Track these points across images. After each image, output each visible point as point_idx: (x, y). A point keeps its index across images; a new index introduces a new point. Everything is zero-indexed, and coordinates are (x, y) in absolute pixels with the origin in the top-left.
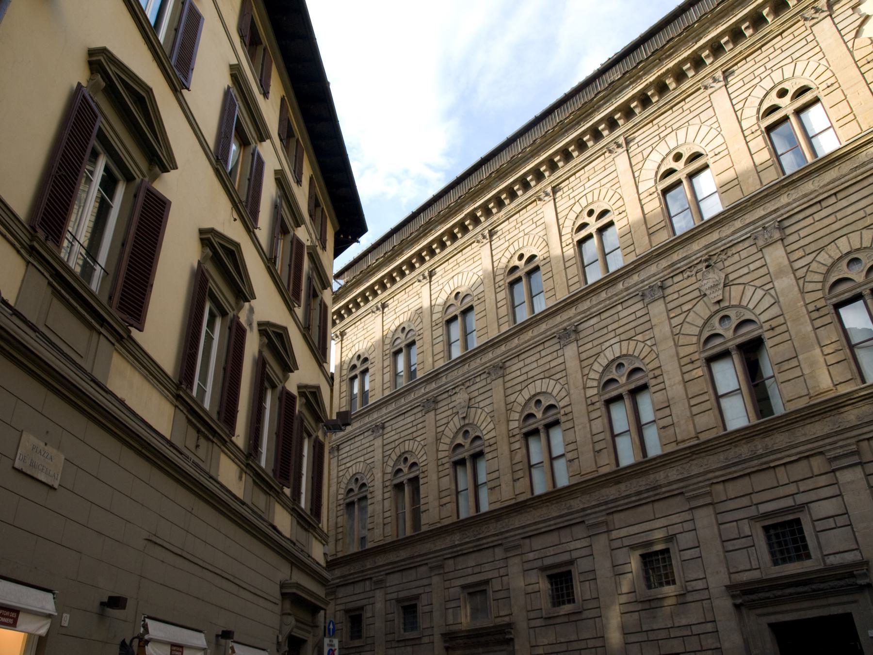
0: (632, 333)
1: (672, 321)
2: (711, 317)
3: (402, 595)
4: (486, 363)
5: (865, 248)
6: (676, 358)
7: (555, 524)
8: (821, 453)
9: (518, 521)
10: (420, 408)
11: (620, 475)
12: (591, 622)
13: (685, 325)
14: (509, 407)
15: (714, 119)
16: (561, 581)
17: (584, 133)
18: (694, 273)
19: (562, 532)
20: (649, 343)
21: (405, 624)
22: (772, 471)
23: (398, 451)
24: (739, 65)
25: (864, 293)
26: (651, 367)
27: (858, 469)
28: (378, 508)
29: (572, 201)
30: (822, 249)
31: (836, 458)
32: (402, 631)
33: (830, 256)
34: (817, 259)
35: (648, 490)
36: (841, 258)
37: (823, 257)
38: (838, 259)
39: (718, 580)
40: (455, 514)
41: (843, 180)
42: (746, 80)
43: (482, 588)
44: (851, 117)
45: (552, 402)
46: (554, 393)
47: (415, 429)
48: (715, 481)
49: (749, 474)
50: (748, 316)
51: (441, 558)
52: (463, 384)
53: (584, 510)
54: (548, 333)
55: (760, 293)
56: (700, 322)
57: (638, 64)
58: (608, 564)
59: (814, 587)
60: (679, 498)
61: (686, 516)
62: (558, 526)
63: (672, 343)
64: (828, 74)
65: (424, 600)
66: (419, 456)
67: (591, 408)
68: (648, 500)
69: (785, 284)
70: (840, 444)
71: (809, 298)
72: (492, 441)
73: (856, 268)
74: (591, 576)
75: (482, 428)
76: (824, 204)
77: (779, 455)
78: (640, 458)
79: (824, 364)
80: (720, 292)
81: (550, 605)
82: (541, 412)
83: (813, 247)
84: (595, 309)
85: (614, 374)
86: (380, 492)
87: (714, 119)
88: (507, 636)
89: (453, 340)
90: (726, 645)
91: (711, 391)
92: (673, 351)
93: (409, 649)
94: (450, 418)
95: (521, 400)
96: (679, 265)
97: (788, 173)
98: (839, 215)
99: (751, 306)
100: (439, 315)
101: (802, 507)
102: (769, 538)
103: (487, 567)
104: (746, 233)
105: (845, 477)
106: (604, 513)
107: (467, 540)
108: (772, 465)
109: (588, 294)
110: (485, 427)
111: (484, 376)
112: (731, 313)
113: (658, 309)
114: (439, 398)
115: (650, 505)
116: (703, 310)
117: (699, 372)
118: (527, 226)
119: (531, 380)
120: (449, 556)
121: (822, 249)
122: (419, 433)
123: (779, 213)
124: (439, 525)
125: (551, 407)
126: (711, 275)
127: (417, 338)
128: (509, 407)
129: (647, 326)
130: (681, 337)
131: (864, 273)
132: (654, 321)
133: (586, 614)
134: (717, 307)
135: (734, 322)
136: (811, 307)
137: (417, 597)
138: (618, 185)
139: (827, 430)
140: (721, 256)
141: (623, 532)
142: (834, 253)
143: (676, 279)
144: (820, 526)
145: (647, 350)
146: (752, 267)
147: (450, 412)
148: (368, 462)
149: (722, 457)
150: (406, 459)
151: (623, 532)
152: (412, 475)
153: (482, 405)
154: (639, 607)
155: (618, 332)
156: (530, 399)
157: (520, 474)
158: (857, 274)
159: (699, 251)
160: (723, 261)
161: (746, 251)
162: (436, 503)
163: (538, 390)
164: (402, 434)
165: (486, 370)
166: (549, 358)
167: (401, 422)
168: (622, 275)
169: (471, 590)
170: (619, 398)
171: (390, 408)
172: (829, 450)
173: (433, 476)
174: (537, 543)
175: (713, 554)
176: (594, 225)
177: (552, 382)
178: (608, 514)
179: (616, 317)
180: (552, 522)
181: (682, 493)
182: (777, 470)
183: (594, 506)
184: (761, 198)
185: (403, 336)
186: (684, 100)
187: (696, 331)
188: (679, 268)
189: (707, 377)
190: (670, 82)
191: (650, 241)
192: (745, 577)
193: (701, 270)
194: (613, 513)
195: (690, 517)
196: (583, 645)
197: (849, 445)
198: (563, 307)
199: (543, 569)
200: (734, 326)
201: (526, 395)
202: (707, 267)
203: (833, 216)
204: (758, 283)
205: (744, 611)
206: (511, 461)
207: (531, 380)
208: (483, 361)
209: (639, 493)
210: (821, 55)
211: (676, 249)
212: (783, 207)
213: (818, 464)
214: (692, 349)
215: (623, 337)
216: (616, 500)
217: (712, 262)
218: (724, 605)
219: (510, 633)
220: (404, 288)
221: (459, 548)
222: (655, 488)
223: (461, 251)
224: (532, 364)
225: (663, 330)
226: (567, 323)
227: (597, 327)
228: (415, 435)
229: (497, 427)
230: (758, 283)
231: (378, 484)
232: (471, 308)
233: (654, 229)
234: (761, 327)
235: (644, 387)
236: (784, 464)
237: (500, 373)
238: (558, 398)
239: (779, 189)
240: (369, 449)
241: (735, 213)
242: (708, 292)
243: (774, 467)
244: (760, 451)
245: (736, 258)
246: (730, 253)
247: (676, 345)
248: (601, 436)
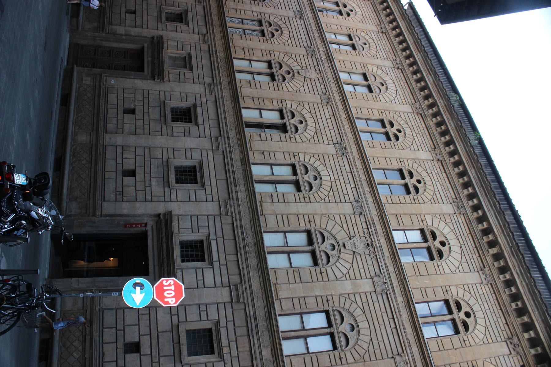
0: (335, 190)
1: (338, 216)
2: (336, 239)
3: (190, 14)
4: (332, 93)
5: (359, 336)
6: (314, 212)
7: (222, 118)
8: (241, 282)
9: (227, 94)
10: (309, 45)
11: (246, 163)
12: (159, 128)
13: (334, 223)
14: (301, 103)
15: (462, 271)
16: (185, 115)
17: (474, 188)
18: (366, 235)
19: (216, 122)
20: (327, 198)
21: (171, 13)
22: (235, 253)
23: (283, 26)
24: (493, 295)
25: (332, 328)
26: (311, 196)
27: (228, 300)
28: (247, 7)
29: (429, 171)
30: (364, 312)
32: (166, 11)
33: (358, 316)
34: (358, 308)
35: (234, 178)
36: (356, 321)
37: (358, 312)
38: (355, 320)
39: (176, 208)
40: (236, 57)
41: (404, 334)
42: (482, 296)
43: (188, 65)
44: (441, 348)
45: (300, 131)
46: (305, 133)
47: (296, 39)
48: (234, 219)
49: (235, 239)
50: (332, 261)
51: (210, 43)
52: (321, 76)
53: (228, 137)
54: (345, 137)
55: (345, 271)
56: (334, 232)
57: (512, 233)
58: (192, 146)
59: (165, 260)
60: (227, 196)
61: (216, 198)
62: (220, 119)
63: (324, 213)
64: (472, 343)
65: (185, 28)
66: (278, 39)
67: (292, 154)
68: (228, 178)
69: (347, 287)
70: (245, 294)
71: (336, 299)
72: (280, 88)
73: (348, 328)
74: (187, 134)
75: (290, 83)
76: (391, 321)
77: (243, 258)
78: (255, 178)
79: (294, 296)
80: (350, 248)
81: (172, 106)
82: (294, 123)
83: (366, 308)
84: (355, 170)
85: (311, 173)
86: (258, 10)
87: (462, 271)
88: (156, 78)
89: (351, 75)
90: (138, 204)
91: (289, 229)
92: (319, 212)
93: (155, 14)
94: (300, 64)
95: (304, 112)
96: (373, 228)
97: (417, 306)
98: (383, 327)
99: (338, 264)
100: (370, 69)
101: (211, 264)
102: (196, 242)
103: (200, 71)
104: (384, 272)
105: (225, 292)
106: (224, 149)
107: (219, 61)
108: (239, 254)
109: (366, 168)
110: (291, 86)
111: (324, 91)
112: (336, 252)
113: (347, 209)
114: (314, 59)
115: (225, 178)
116: (341, 236)
117: (302, 224)
118: (419, 139)
119: (316, 121)
120: (211, 48)
121: (364, 312)
122: (293, 42)
123: (392, 294)
124: (231, 45)
125: (297, 130)
126: (362, 245)
127: (357, 52)
128: (301, 103)
129: (338, 200)
130: (327, 219)
131: (344, 332)
132: (340, 204)
133: (164, 127)
135: (330, 252)
136: (329, 298)
137: (187, 24)
138: (433, 202)
139: (254, 288)
140: (373, 254)
141: (211, 159)
142: (361, 319)
143: (364, 224)
144: (199, 272)
145: (323, 197)
146: (362, 271)
147: (304, 64)
148: (279, 5)
149: (248, 226)
150: (277, 30)
151: (211, 159)
152: (266, 32)
153: (306, 86)
154: (165, 160)
155: (338, 182)
156: (304, 117)
157: (256, 102)
158: (345, 327)
159: (379, 242)
160: (369, 254)
161: (372, 269)
162: (245, 45)
163: (309, 124)
164: (294, 31)
165: (327, 93)
166: (329, 135)
167: (302, 31)
168: (374, 191)
169: (187, 59)
170: (295, 173)
171: (313, 25)
172: (242, 287)
173: (264, 46)
174: (211, 106)
175: (190, 208)
176: (411, 182)
177: (312, 134)
178: (223, 152)
179: (347, 182)
180: (223, 116)
181: (229, 198)
182: (235, 256)
183: (229, 144)
184: (404, 286)
185: (360, 43)
186: (480, 256)
187: (329, 228)
188: (371, 227)
189: (299, 229)
190: (495, 250)
191: (392, 214)
192: (175, 224)
193: (367, 240)
194: (224, 154)
195: (214, 200)
196: (146, 122)
197: (244, 298)
198: (360, 151)
199: (195, 105)
200: (327, 251)
201: (307, 116)
202: (368, 244)
203: (383, 323)
204: (351, 272)
205: (156, 219)
206: (267, 98)
207: (316, 121)
208: (334, 92)
209: (233, 173)
210: (486, 342)
211: (384, 228)
212: (395, 296)
213: (235, 279)
214: (318, 223)
215: (333, 184)
216: (231, 157)
217: (370, 247)
218: (161, 208)
219: (158, 79)
220: (393, 49)
221: (214, 55)
222: (235, 182)
223: (411, 93)
224: (327, 123)
225: (333, 209)
226: (349, 150)
227: (343, 168)
228: (293, 39)
229: (290, 93)
230: (351, 272)
231: (263, 9)
232: (371, 91)
233: (399, 218)
234: (323, 267)
235: (299, 189)
236: (238, 261)
237: (325, 102)
238: (301, 135)
239: (407, 297)
240: (287, 7)
241: (398, 268)
242: (352, 241)
243: (237, 254)
244: (248, 249)
245: (370, 263)
246: (373, 259)
247: (322, 215)
248: (272, 157)
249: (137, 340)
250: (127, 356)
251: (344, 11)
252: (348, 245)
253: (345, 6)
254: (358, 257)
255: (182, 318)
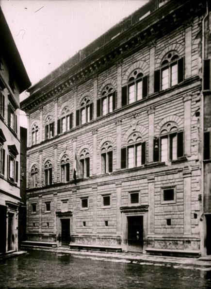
31: (150, 180)
116: (131, 131)
121: (163, 119)
134: (133, 131)
161: (144, 114)
249: (166, 221)
250: (172, 223)
251: (35, 129)
252: (133, 128)
253: (33, 129)
254: (139, 122)
255: (159, 202)
